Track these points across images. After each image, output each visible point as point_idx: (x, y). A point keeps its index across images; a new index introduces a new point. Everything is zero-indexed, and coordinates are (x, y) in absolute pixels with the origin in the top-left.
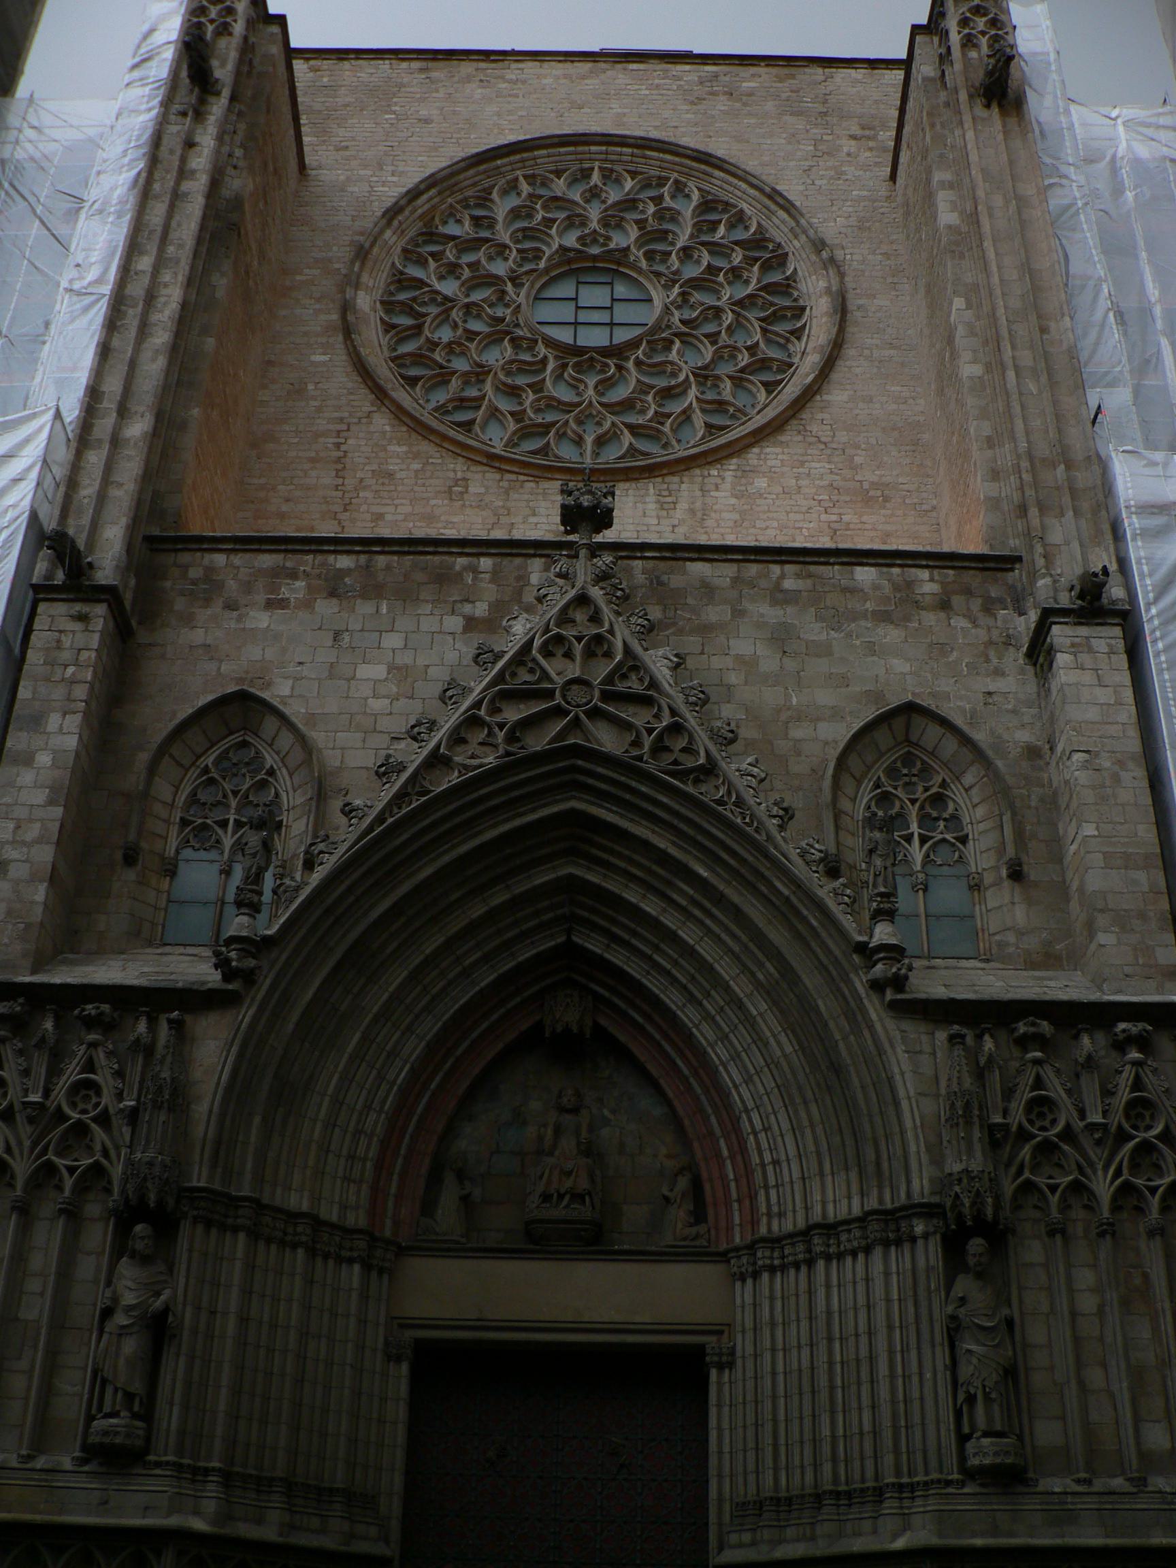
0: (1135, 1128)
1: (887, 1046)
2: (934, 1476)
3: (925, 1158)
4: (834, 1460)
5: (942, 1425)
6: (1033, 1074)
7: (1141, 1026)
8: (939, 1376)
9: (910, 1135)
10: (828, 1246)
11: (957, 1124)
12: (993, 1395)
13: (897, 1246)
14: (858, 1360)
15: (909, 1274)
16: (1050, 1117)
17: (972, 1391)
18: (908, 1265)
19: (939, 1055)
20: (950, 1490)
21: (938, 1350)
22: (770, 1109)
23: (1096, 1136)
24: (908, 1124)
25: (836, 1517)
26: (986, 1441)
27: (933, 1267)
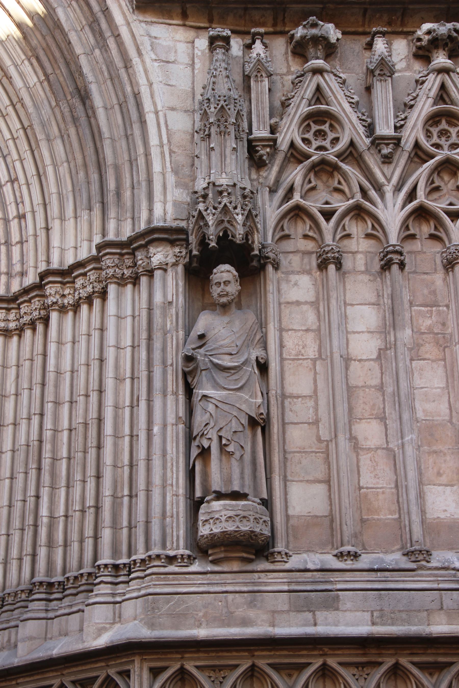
0: (437, 146)
1: (132, 53)
2: (155, 551)
3: (171, 179)
4: (50, 544)
5: (169, 488)
6: (313, 87)
7: (450, 26)
8: (169, 428)
9: (155, 152)
10: (64, 296)
11: (209, 135)
12: (230, 449)
13: (134, 284)
14: (86, 424)
15: (144, 313)
16: (331, 135)
17: (206, 444)
18: (144, 305)
19: (198, 65)
20: (172, 568)
21: (170, 399)
22: (15, 156)
23: (385, 151)
24: (154, 140)
25: (43, 615)
26: (217, 505)
27: (170, 303)
